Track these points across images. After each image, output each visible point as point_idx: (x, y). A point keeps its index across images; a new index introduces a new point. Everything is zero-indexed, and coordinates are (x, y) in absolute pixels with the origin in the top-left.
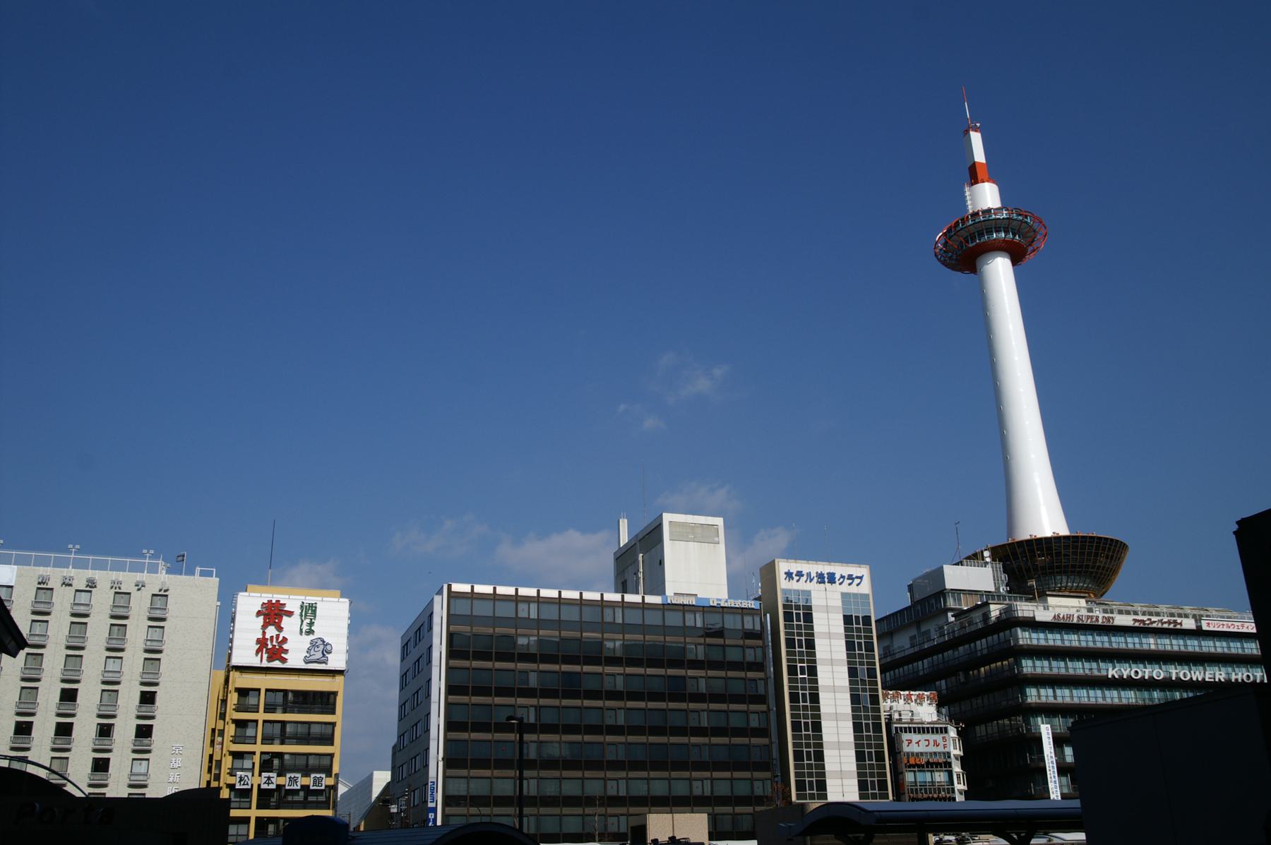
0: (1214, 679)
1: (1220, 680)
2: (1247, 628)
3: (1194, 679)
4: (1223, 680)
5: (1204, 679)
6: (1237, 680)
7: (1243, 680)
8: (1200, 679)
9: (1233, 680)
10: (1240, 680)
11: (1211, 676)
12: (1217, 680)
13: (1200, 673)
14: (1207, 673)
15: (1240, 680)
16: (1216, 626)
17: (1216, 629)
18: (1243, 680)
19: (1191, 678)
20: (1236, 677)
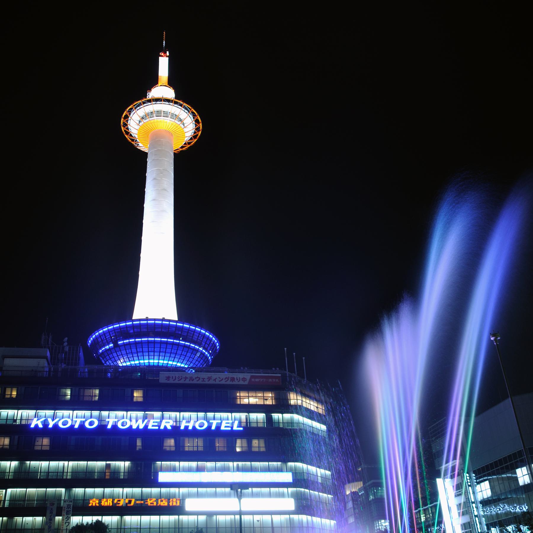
0: (159, 426)
1: (165, 427)
2: (215, 380)
3: (134, 427)
4: (169, 428)
5: (146, 426)
6: (186, 427)
7: (194, 427)
8: (141, 427)
9: (182, 428)
10: (190, 428)
11: (156, 424)
12: (162, 427)
13: (143, 421)
14: (152, 421)
15: (190, 428)
16: (177, 379)
17: (176, 381)
18: (194, 427)
19: (131, 426)
20: (187, 424)
